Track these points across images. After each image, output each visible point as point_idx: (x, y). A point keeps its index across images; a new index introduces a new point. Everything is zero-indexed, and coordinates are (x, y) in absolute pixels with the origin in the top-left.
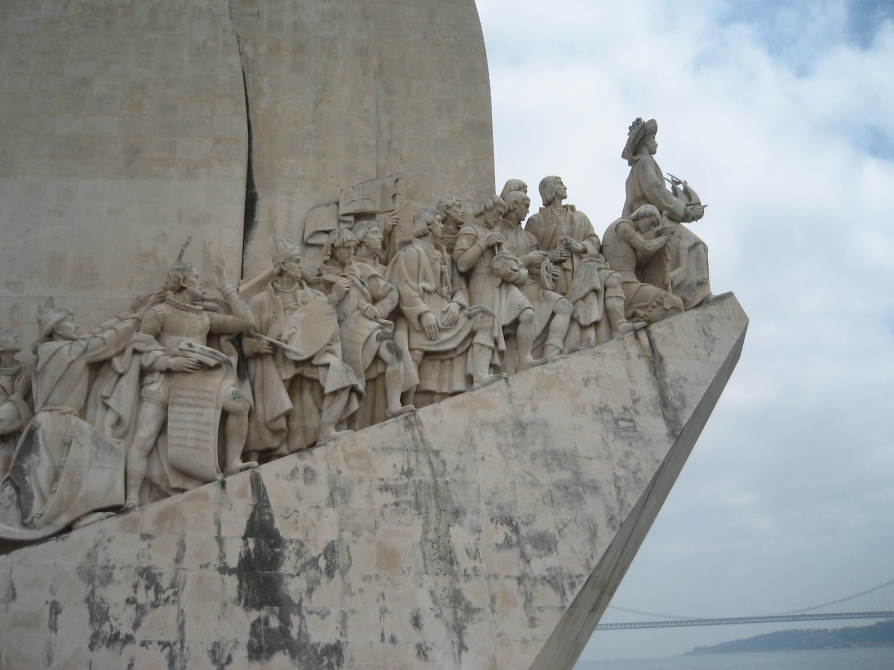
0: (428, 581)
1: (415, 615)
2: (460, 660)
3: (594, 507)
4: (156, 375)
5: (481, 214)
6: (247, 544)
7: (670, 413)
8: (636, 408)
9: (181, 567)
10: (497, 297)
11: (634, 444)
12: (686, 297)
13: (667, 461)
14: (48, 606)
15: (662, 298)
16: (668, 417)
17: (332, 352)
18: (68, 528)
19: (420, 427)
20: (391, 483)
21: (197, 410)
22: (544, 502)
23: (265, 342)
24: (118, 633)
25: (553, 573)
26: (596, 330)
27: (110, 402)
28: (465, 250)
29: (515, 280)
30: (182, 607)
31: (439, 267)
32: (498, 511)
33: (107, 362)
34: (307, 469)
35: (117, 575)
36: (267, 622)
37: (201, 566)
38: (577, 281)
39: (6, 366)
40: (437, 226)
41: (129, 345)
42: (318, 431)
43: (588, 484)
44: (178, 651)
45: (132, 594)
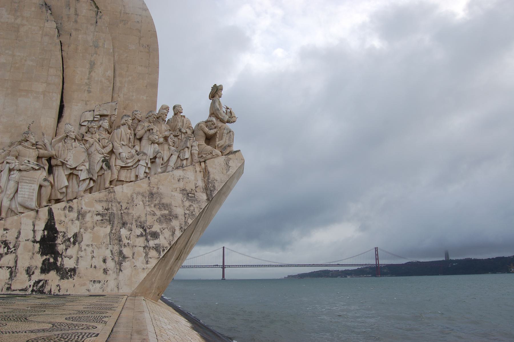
0: (110, 247)
1: (104, 259)
2: (119, 275)
3: (175, 223)
4: (15, 171)
5: (147, 118)
6: (44, 233)
7: (209, 192)
8: (196, 190)
9: (18, 241)
10: (150, 148)
11: (193, 202)
12: (223, 151)
13: (206, 209)
16: (208, 193)
17: (84, 165)
19: (114, 193)
20: (101, 213)
21: (30, 185)
22: (157, 221)
23: (59, 161)
25: (157, 246)
26: (187, 161)
28: (139, 131)
29: (158, 142)
30: (17, 255)
31: (128, 136)
32: (140, 224)
34: (70, 207)
36: (49, 259)
38: (183, 143)
40: (129, 121)
42: (77, 193)
43: (174, 216)
44: (14, 270)
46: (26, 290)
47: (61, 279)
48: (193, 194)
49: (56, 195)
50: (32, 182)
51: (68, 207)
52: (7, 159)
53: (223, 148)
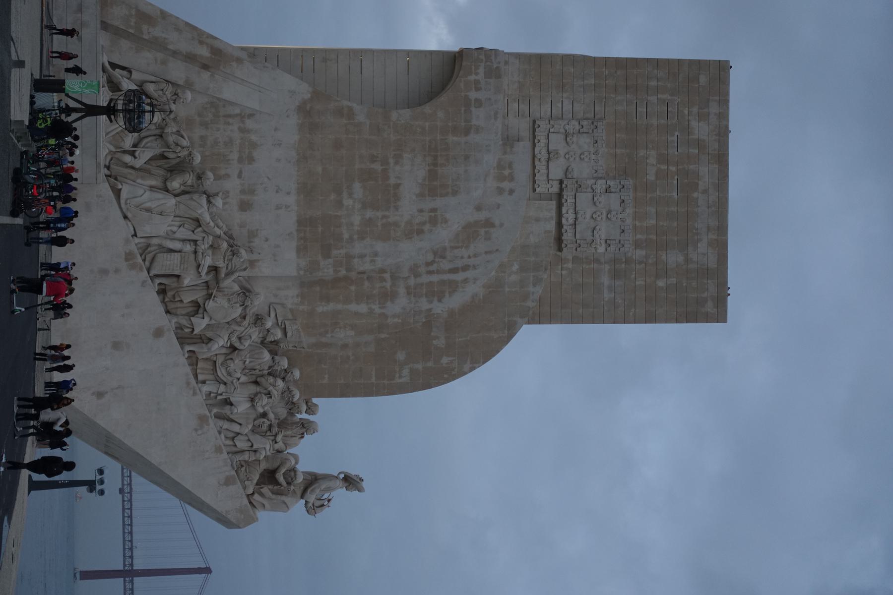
4: (194, 247)
15: (250, 480)
17: (211, 319)
18: (125, 217)
27: (181, 228)
31: (258, 367)
33: (200, 226)
38: (258, 436)
39: (196, 182)
41: (208, 235)
42: (176, 315)
49: (171, 290)
50: (182, 267)
52: (208, 237)
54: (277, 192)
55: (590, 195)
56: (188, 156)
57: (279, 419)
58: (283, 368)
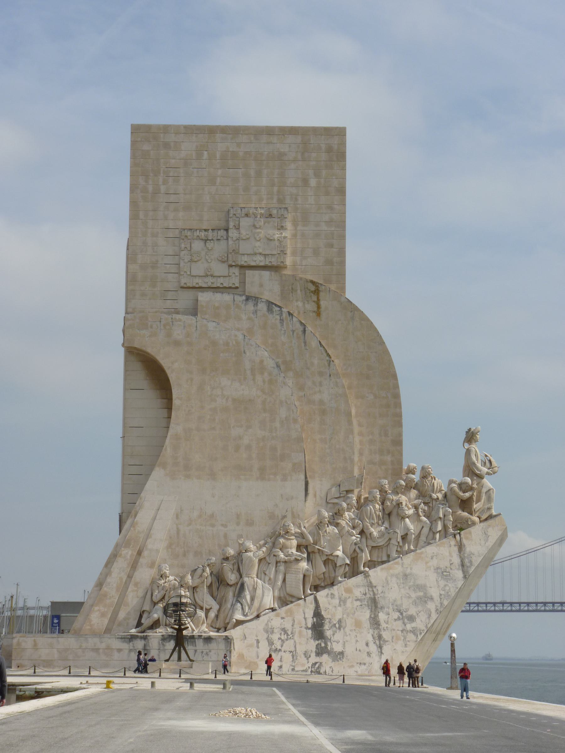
3: (431, 606)
4: (281, 563)
6: (314, 620)
14: (256, 641)
15: (468, 520)
20: (360, 598)
21: (295, 575)
22: (413, 604)
24: (277, 648)
25: (414, 629)
27: (267, 573)
33: (265, 558)
35: (275, 631)
36: (321, 644)
37: (300, 627)
40: (377, 497)
42: (335, 578)
45: (280, 636)
46: (307, 671)
47: (332, 661)
48: (447, 572)
51: (330, 594)
53: (481, 512)
54: (238, 496)
55: (241, 242)
56: (210, 567)
57: (419, 496)
58: (378, 493)
